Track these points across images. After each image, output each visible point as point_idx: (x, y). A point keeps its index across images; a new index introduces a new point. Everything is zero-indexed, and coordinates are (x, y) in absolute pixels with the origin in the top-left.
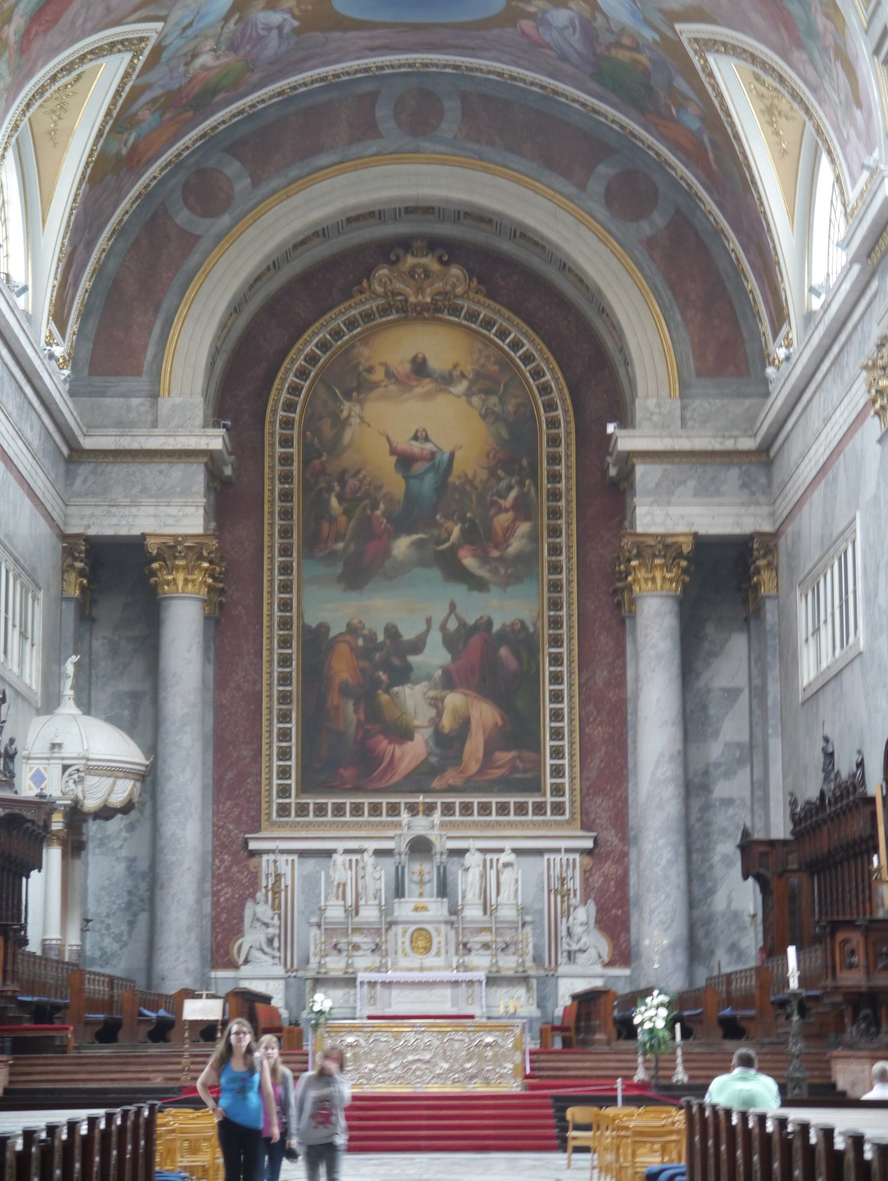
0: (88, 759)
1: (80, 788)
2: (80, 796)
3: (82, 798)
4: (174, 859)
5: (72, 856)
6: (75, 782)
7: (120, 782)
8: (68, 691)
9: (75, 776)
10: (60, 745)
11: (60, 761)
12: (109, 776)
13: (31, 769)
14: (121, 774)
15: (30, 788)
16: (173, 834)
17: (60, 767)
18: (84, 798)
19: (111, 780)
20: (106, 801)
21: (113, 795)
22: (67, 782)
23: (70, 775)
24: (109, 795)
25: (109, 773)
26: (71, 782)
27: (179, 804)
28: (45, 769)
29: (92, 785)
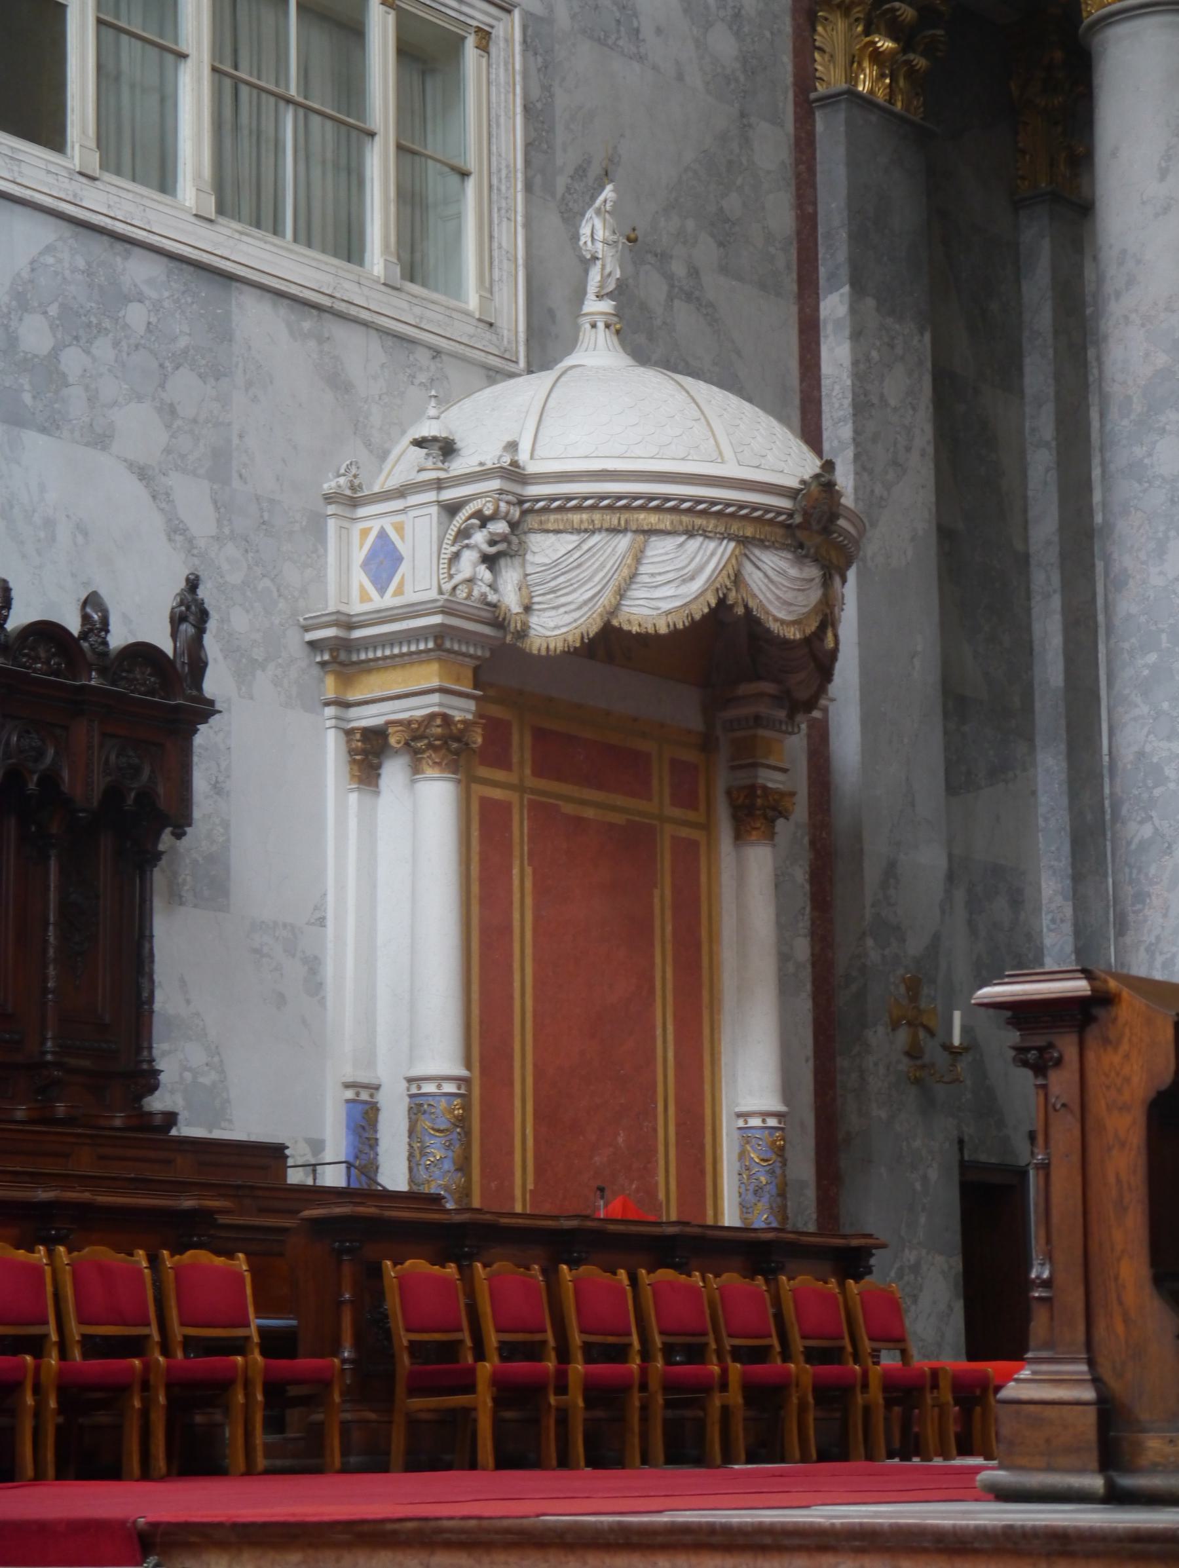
0: (514, 473)
1: (510, 577)
2: (511, 600)
3: (516, 608)
4: (1147, 831)
5: (739, 836)
6: (490, 561)
7: (662, 550)
8: (596, 307)
9: (479, 538)
10: (447, 449)
11: (431, 496)
12: (614, 531)
13: (365, 533)
14: (666, 521)
15: (365, 597)
16: (1141, 754)
17: (434, 510)
18: (528, 609)
19: (623, 542)
20: (614, 611)
21: (637, 593)
22: (456, 556)
23: (464, 533)
24: (621, 593)
25: (613, 519)
26: (469, 559)
27: (1152, 658)
28: (399, 528)
29: (556, 564)
